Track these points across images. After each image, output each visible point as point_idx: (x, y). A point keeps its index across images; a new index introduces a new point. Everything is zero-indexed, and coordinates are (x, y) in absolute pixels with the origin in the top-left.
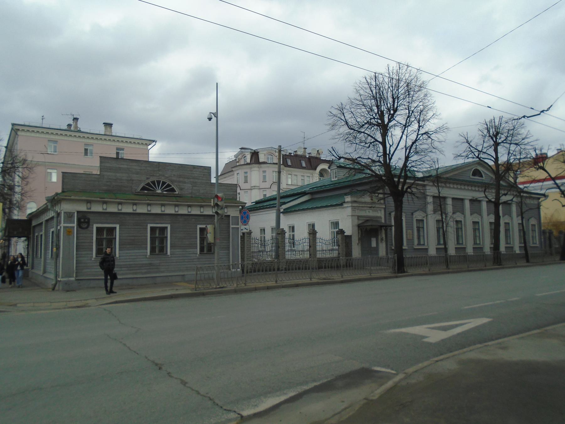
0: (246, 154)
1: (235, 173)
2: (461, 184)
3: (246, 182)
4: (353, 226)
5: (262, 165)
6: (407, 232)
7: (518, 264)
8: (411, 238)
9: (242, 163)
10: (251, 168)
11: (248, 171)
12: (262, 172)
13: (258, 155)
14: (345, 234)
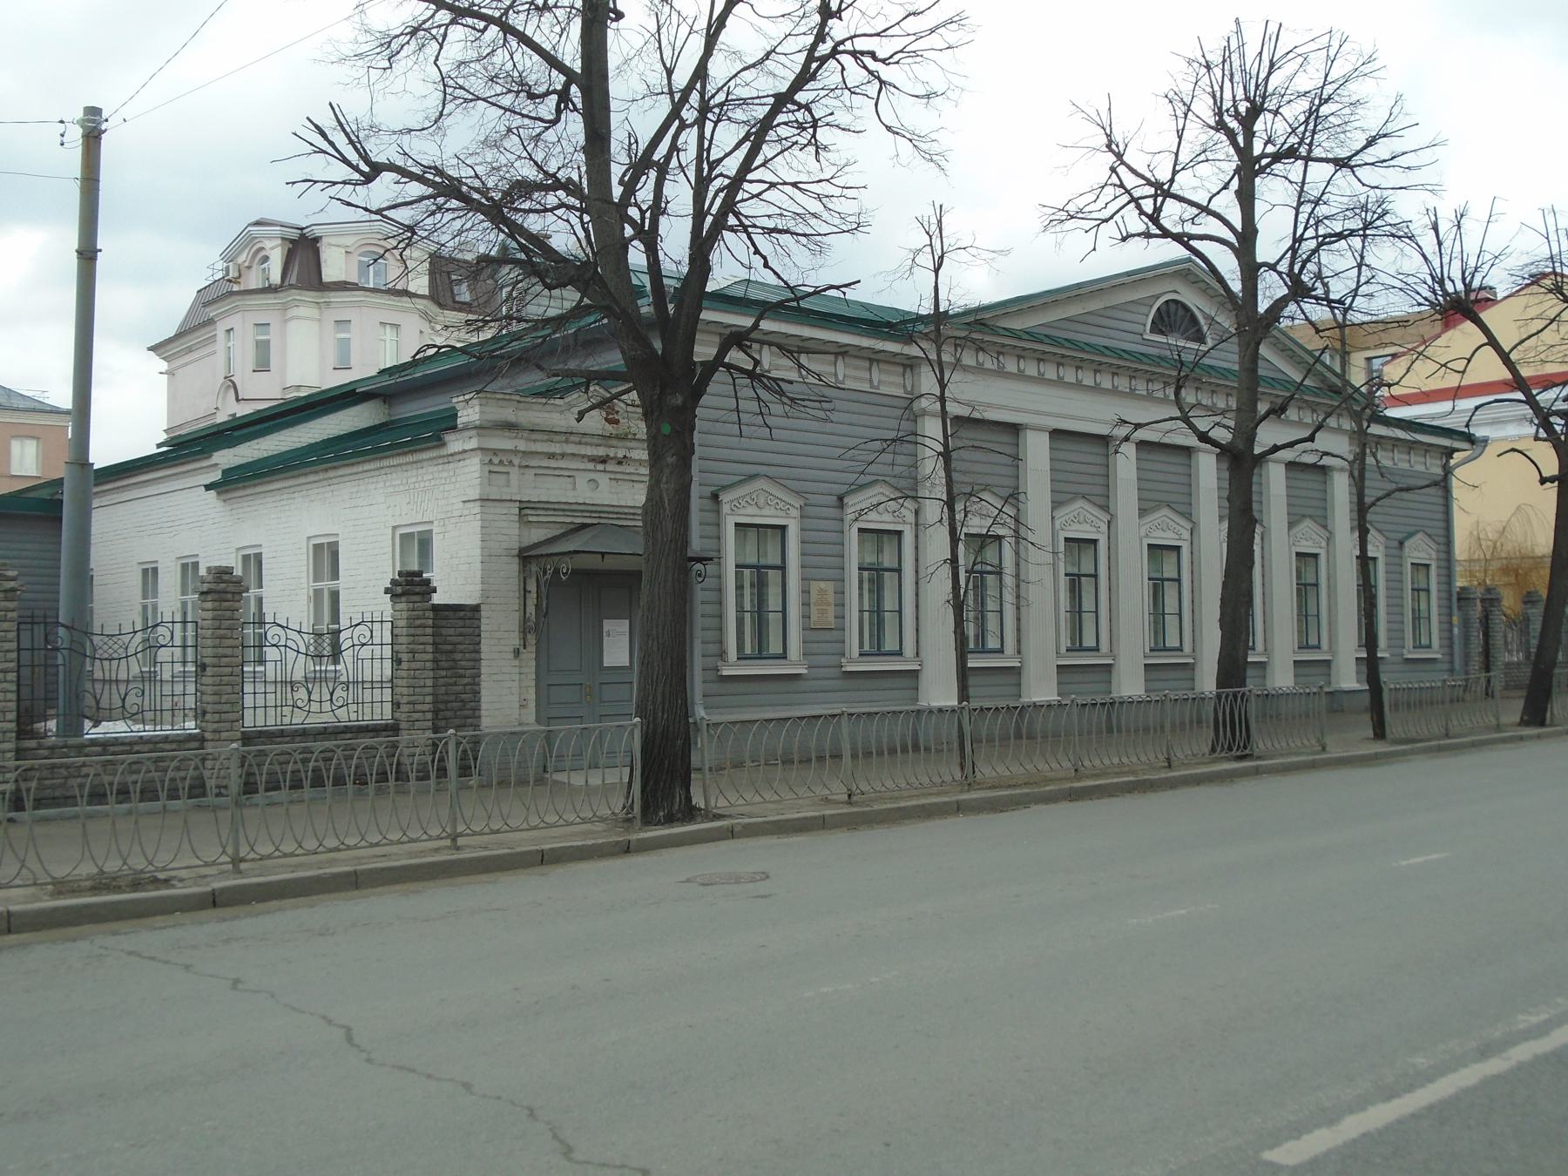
0: (268, 244)
1: (221, 327)
2: (1098, 369)
3: (263, 365)
4: (488, 557)
5: (336, 297)
6: (806, 592)
7: (1335, 752)
8: (830, 620)
9: (253, 286)
10: (285, 308)
11: (272, 318)
12: (330, 326)
13: (317, 253)
14: (437, 599)
